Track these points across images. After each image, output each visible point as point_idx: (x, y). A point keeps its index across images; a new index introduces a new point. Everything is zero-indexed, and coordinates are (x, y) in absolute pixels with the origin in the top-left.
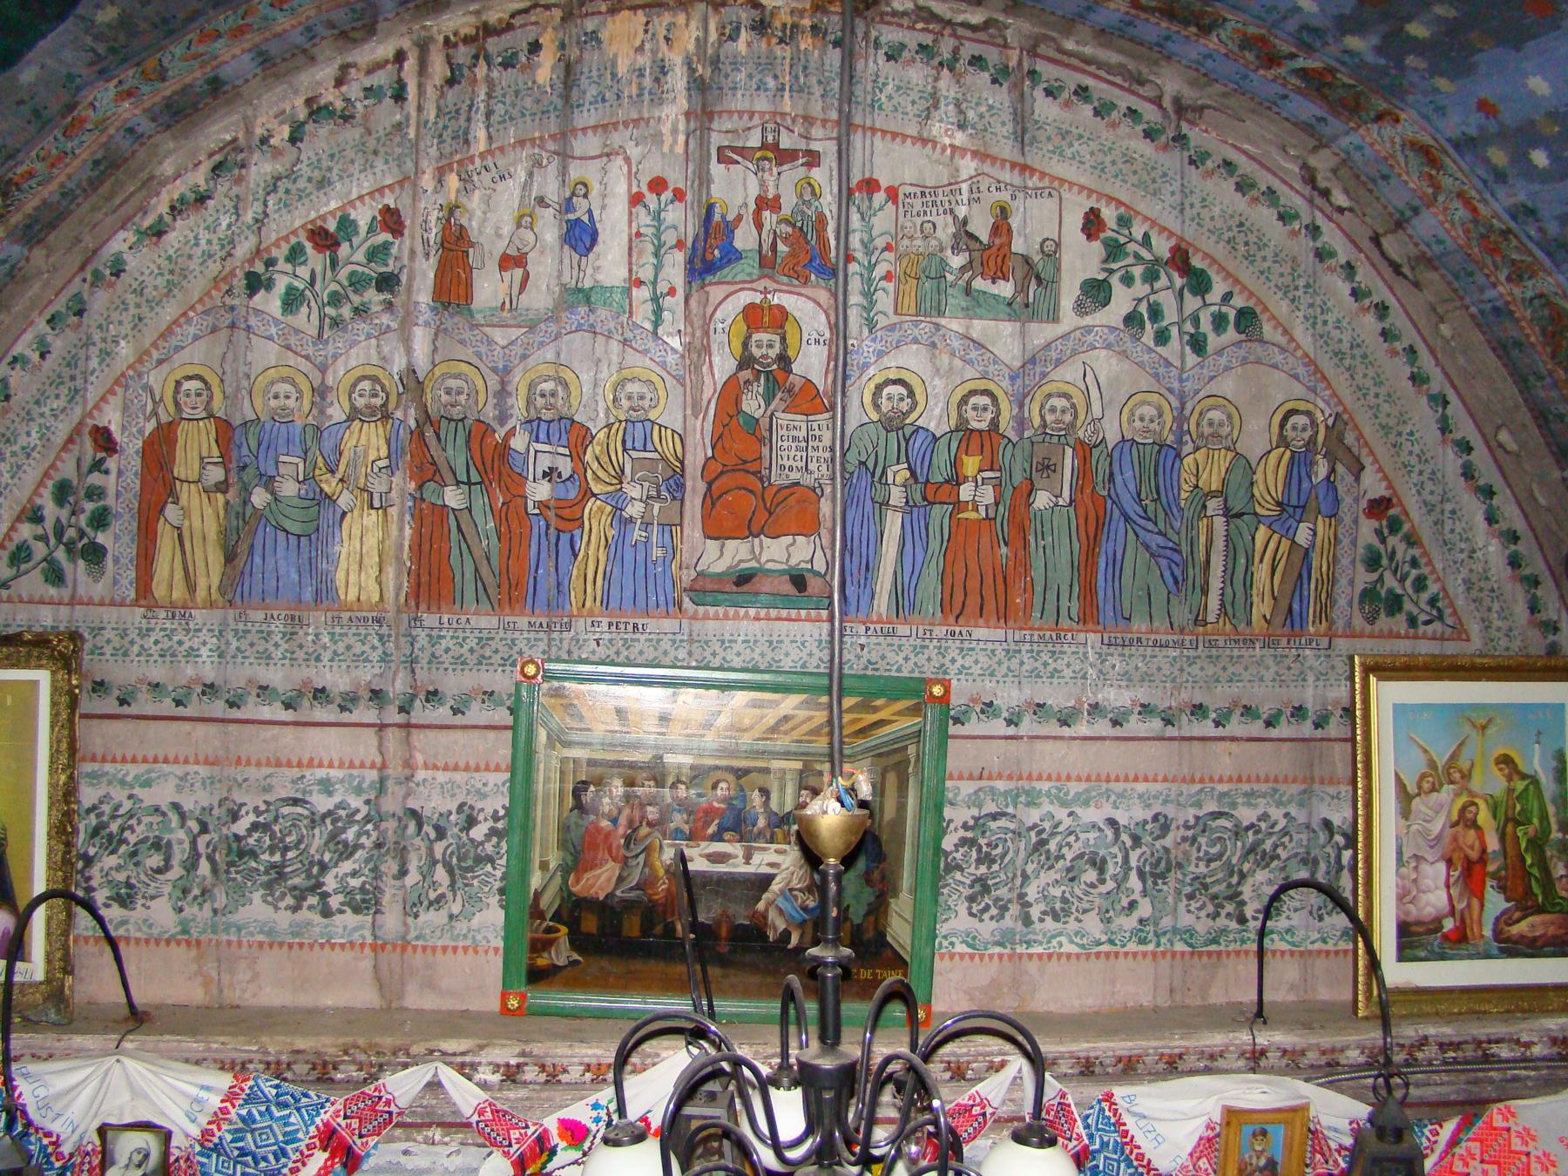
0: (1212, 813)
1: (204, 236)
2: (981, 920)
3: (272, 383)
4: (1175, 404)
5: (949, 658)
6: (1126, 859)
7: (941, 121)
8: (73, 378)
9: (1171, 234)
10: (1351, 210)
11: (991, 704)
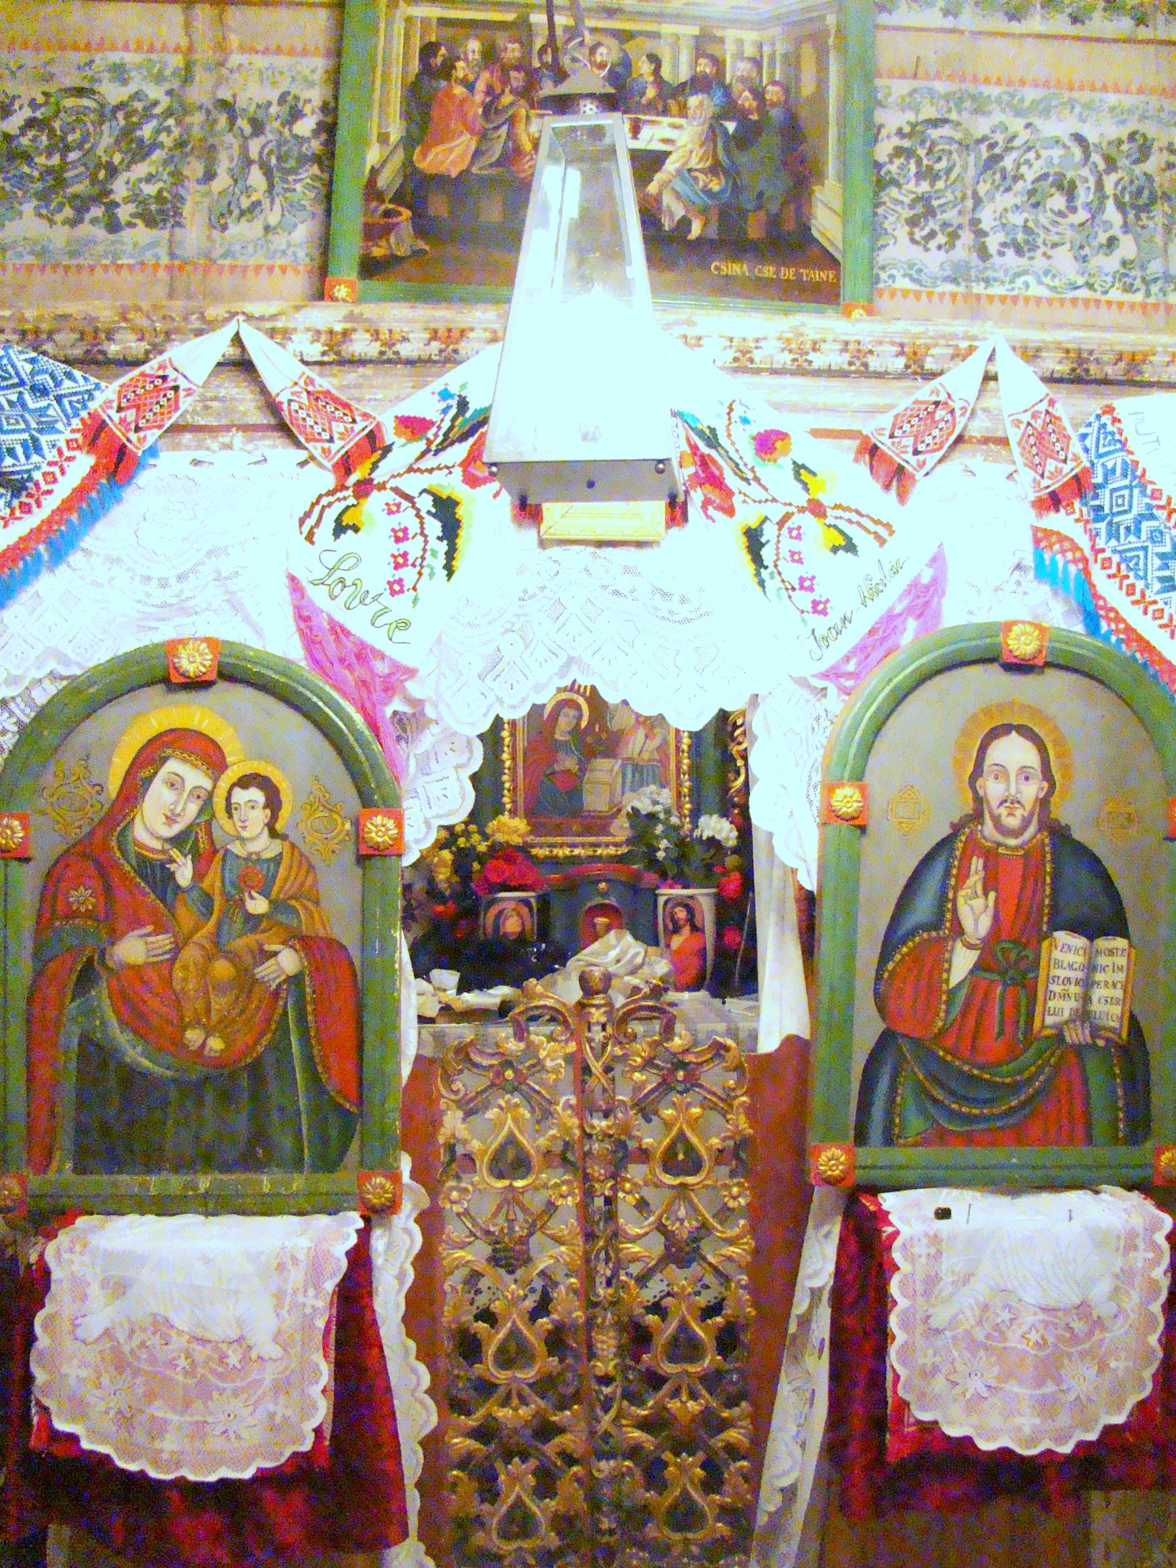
2: (926, 249)
6: (1100, 185)
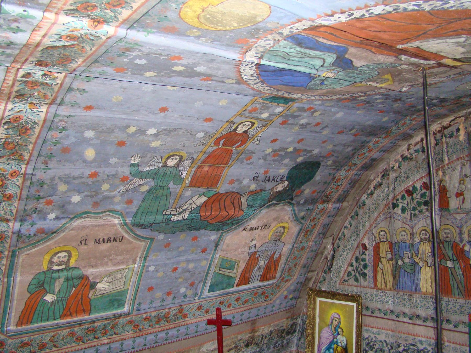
1: (382, 194)
8: (357, 231)
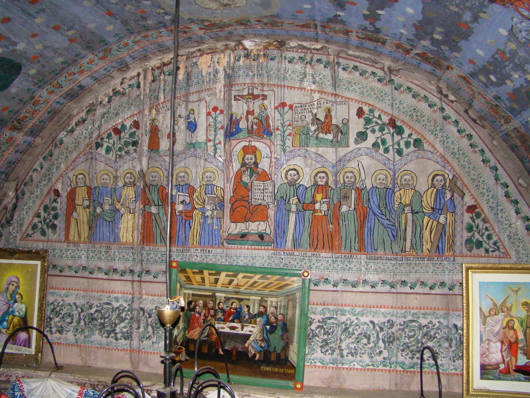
0: (410, 320)
1: (84, 132)
2: (326, 355)
3: (102, 175)
4: (392, 173)
5: (312, 263)
6: (378, 336)
7: (307, 82)
8: (49, 175)
9: (389, 114)
10: (456, 101)
11: (327, 279)
